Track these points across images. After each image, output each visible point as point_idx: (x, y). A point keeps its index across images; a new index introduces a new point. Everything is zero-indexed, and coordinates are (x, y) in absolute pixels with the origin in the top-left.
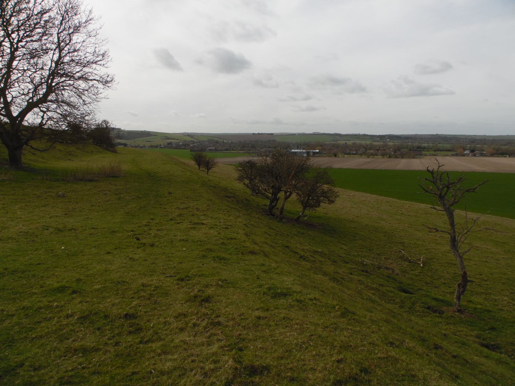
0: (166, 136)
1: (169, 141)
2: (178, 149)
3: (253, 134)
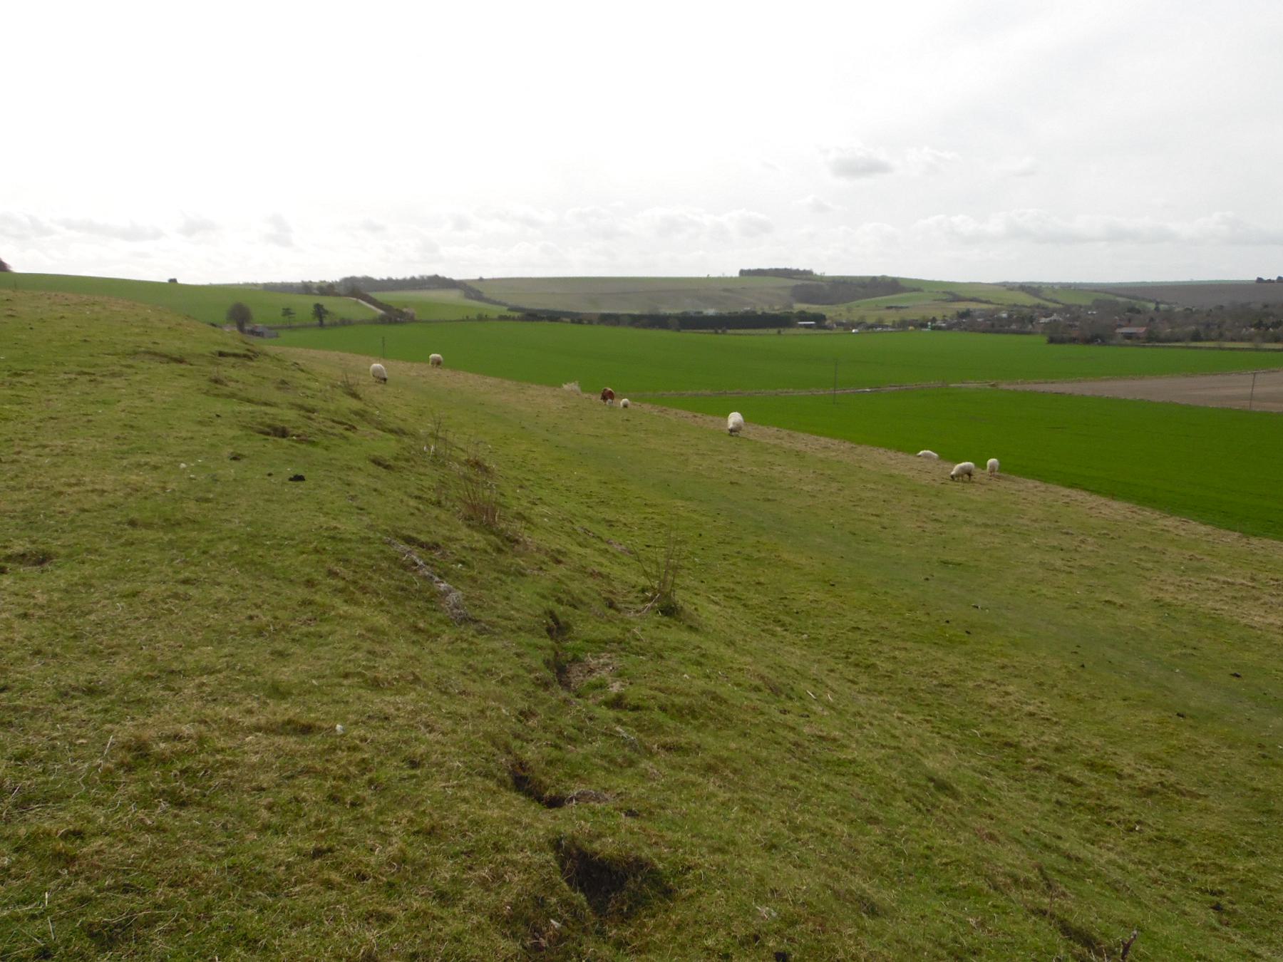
0: (951, 293)
1: (962, 306)
2: (998, 332)
3: (1260, 280)
